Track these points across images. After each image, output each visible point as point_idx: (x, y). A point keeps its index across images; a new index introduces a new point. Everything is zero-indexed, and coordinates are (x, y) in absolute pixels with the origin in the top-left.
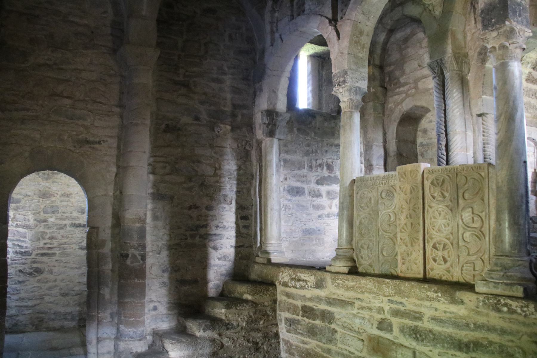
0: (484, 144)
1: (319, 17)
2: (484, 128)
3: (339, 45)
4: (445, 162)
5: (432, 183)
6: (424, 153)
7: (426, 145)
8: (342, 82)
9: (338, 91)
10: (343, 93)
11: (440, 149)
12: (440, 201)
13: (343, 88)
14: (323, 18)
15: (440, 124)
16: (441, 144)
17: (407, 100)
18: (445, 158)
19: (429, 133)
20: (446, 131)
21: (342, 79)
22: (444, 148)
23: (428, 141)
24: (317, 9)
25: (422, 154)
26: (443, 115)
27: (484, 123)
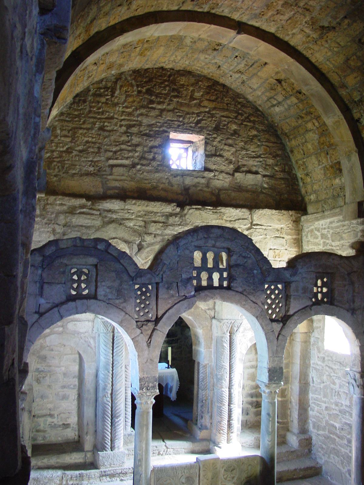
0: (126, 387)
1: (123, 314)
2: (126, 375)
3: (149, 351)
4: (110, 409)
5: (225, 470)
6: (41, 379)
7: (42, 371)
8: (152, 387)
9: (145, 394)
10: (150, 397)
11: (106, 397)
12: (229, 480)
13: (151, 392)
14: (127, 316)
15: (108, 376)
16: (107, 392)
17: (53, 336)
18: (110, 404)
19: (48, 361)
20: (112, 382)
21: (151, 385)
22: (110, 396)
23: (46, 369)
24: (117, 301)
25: (38, 379)
26: (111, 369)
27: (127, 370)
